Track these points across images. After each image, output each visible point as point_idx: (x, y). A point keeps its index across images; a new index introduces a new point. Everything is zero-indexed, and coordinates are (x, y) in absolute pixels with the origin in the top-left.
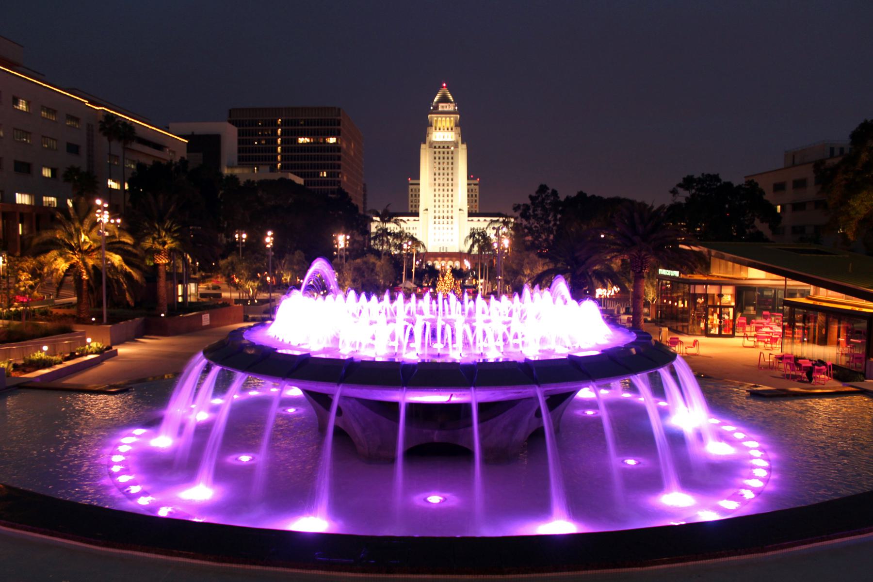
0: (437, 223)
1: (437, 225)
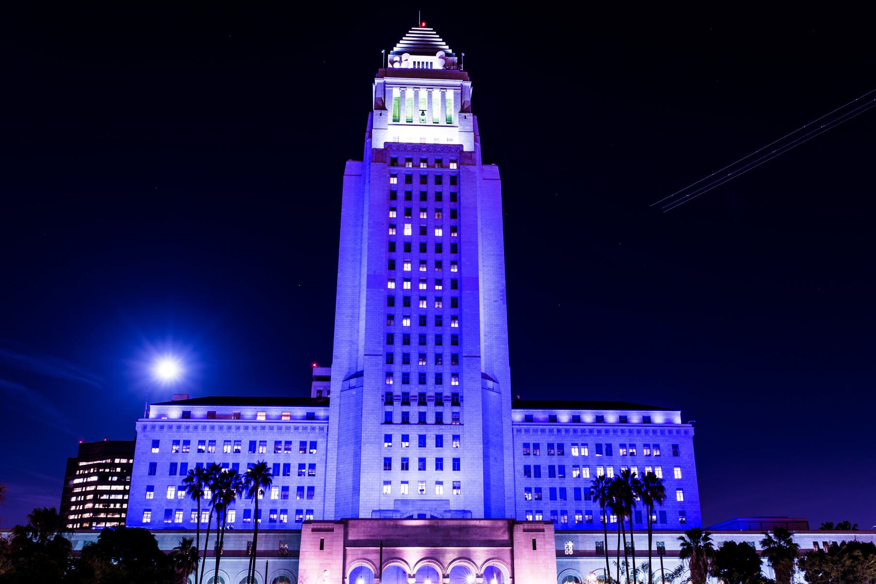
0: (397, 418)
1: (397, 432)
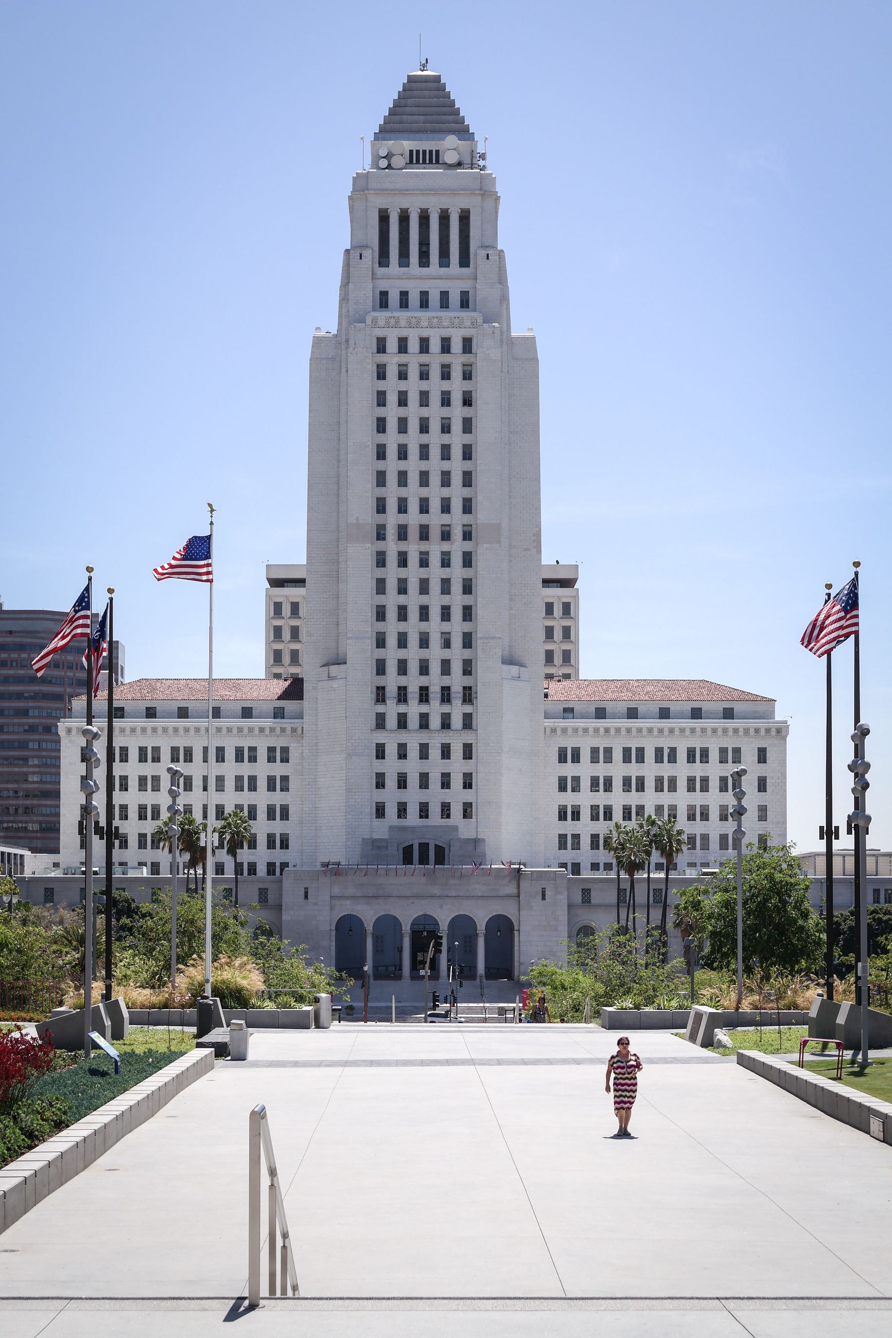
1: (391, 740)
